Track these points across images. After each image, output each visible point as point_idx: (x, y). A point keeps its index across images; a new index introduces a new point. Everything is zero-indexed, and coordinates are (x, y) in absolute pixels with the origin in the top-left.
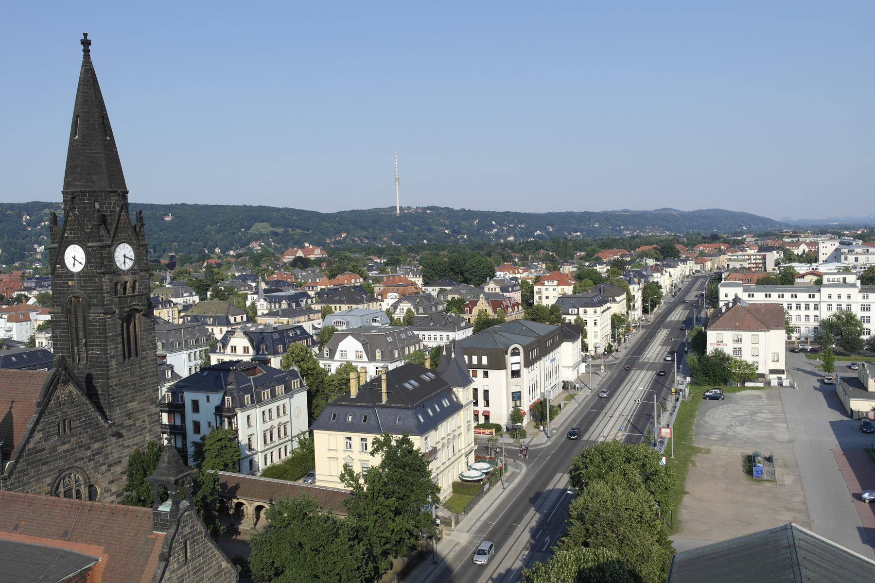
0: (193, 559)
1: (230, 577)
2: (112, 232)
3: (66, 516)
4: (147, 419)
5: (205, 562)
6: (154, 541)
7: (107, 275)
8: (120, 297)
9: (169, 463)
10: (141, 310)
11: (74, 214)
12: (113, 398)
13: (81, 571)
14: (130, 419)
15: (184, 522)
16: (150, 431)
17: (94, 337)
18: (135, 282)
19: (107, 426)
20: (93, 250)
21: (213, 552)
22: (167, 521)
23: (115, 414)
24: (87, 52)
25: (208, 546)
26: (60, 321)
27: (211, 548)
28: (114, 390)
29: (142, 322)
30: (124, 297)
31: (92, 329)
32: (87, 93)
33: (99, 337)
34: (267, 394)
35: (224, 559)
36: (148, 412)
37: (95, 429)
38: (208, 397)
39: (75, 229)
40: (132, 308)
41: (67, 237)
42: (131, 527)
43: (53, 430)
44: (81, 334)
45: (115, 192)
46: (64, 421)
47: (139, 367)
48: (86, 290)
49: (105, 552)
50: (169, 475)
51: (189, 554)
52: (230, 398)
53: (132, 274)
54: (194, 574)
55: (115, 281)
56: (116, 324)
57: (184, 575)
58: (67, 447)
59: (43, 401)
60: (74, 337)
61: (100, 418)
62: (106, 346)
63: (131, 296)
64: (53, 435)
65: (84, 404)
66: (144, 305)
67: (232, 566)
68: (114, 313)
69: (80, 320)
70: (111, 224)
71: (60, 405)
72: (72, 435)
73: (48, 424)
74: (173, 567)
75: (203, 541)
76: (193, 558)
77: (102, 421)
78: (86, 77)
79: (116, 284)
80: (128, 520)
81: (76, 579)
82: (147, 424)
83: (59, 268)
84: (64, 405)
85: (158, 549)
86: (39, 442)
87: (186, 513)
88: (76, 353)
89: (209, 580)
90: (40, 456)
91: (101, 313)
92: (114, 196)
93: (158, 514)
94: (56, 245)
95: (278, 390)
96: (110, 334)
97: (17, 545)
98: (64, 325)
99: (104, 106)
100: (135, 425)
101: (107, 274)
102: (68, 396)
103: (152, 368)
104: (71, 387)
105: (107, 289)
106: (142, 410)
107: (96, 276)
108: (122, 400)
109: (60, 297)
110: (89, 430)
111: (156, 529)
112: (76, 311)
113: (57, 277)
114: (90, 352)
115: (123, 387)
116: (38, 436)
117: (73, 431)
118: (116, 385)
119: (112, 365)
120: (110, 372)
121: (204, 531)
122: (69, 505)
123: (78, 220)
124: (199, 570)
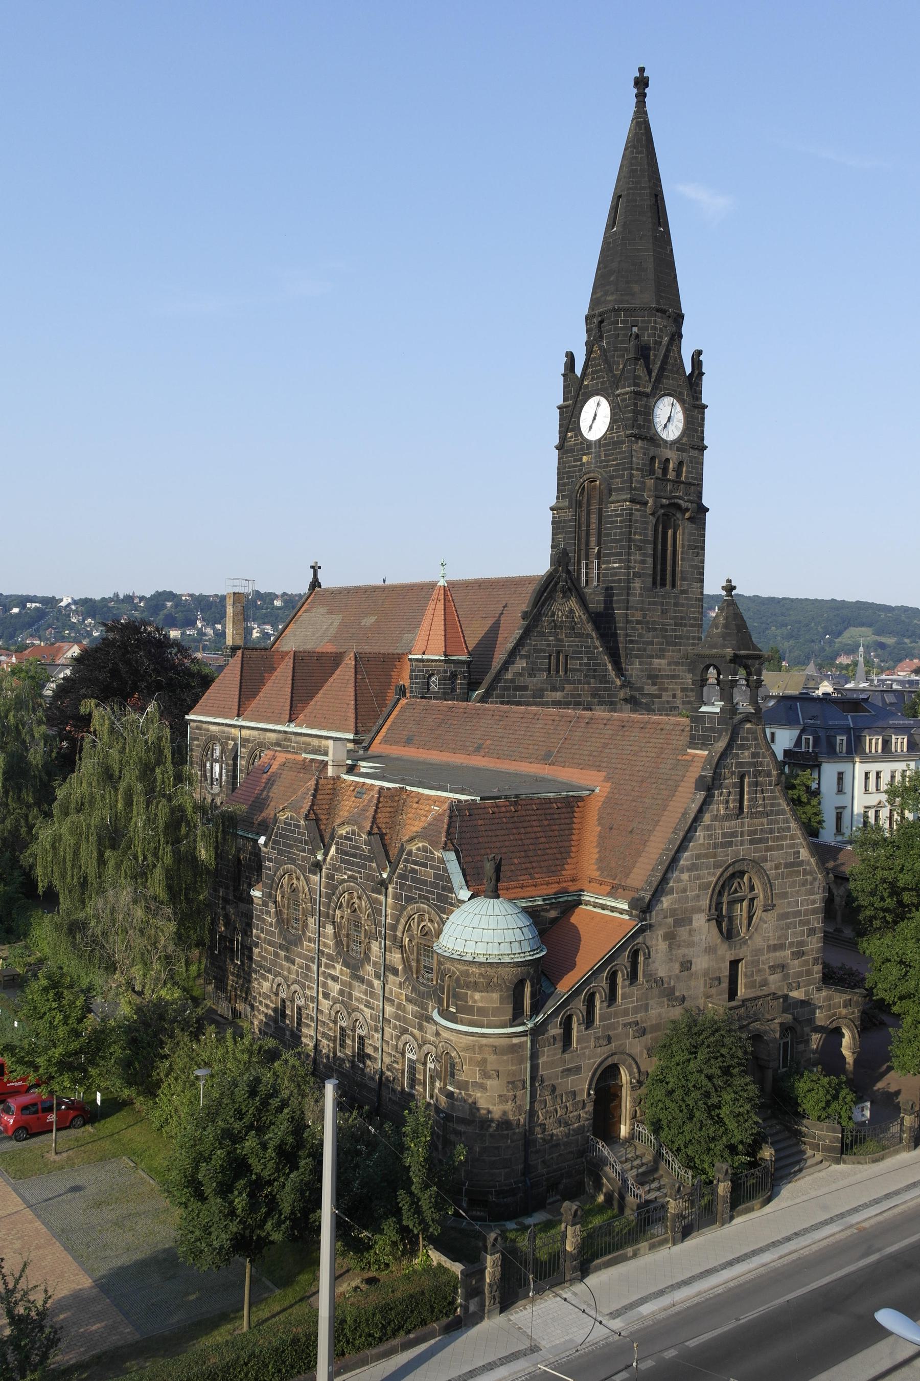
0: (753, 815)
1: (811, 883)
2: (654, 374)
3: (551, 731)
4: (679, 694)
5: (771, 831)
6: (688, 764)
7: (640, 441)
8: (657, 478)
9: (726, 626)
10: (687, 510)
11: (600, 348)
12: (632, 642)
13: (568, 797)
14: (654, 684)
17: (612, 541)
18: (681, 464)
19: (618, 683)
20: (623, 400)
21: (786, 821)
22: (713, 730)
23: (632, 669)
24: (641, 97)
25: (779, 805)
26: (565, 521)
27: (783, 812)
28: (634, 629)
29: (686, 531)
30: (663, 479)
31: (611, 528)
32: (636, 158)
33: (618, 541)
34: (877, 744)
35: (804, 843)
36: (682, 683)
37: (601, 682)
39: (600, 370)
40: (673, 501)
41: (587, 386)
42: (651, 745)
43: (542, 663)
44: (593, 539)
45: (663, 312)
46: (558, 653)
47: (676, 605)
48: (607, 466)
49: (607, 779)
50: (725, 646)
51: (746, 803)
52: (811, 738)
53: (678, 449)
55: (651, 454)
56: (646, 523)
57: (733, 834)
59: (532, 611)
60: (583, 546)
61: (610, 667)
62: (629, 554)
63: (673, 481)
64: (540, 669)
65: (588, 636)
66: (691, 502)
67: (817, 864)
68: (645, 504)
69: (594, 518)
70: (655, 363)
71: (556, 626)
72: (568, 681)
73: (536, 651)
74: (718, 810)
75: (773, 791)
76: (752, 813)
77: (613, 673)
78: (636, 134)
79: (653, 459)
80: (648, 735)
81: (559, 805)
82: (678, 702)
83: (571, 437)
84: (561, 628)
85: (695, 772)
86: (520, 675)
87: (748, 725)
88: (584, 570)
89: (777, 867)
90: (520, 696)
91: (625, 501)
92: (662, 318)
93: (698, 719)
94: (570, 402)
95: (896, 743)
96: (637, 537)
97: (476, 770)
98: (570, 527)
99: (659, 180)
100: (660, 697)
101: (643, 439)
102: (567, 617)
103: (694, 613)
104: (573, 603)
105: (638, 464)
106: (673, 677)
107: (623, 442)
108: (645, 650)
109: (568, 484)
110: (592, 680)
111: (693, 745)
112: (589, 504)
113: (567, 452)
114: (603, 566)
116: (520, 664)
117: (570, 674)
118: (638, 622)
119: (634, 588)
120: (631, 598)
121: (774, 773)
122: (557, 718)
123: (606, 356)
124: (760, 841)
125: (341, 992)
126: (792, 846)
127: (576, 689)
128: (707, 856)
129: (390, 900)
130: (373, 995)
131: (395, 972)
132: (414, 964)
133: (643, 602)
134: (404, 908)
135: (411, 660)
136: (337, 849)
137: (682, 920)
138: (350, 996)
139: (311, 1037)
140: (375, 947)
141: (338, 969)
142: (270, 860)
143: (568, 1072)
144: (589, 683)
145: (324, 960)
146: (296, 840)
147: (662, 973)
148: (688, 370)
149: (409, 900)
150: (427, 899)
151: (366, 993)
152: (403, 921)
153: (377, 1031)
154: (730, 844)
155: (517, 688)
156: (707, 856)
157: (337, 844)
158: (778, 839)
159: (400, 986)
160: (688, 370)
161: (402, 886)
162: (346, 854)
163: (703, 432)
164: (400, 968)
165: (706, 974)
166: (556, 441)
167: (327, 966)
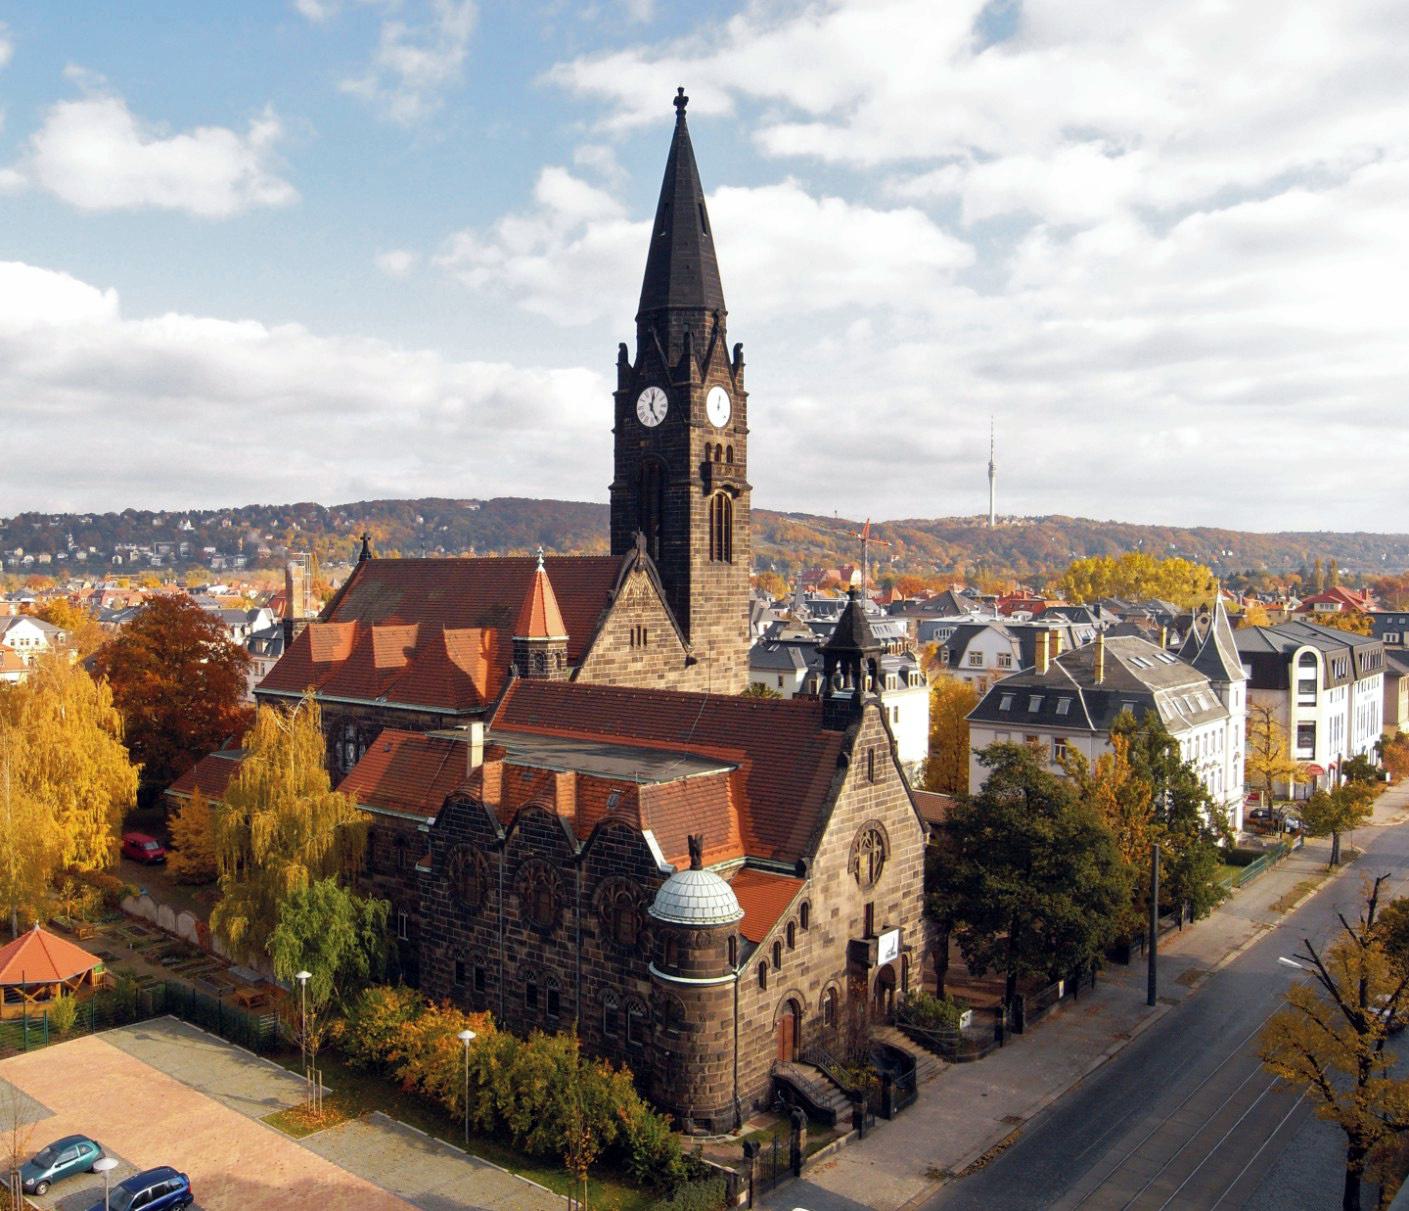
4: (733, 657)
15: (870, 720)
16: (736, 675)
38: (780, 679)
41: (644, 377)
47: (729, 575)
53: (728, 435)
54: (877, 805)
55: (706, 440)
57: (865, 800)
58: (638, 666)
73: (621, 627)
82: (732, 664)
86: (609, 649)
89: (893, 824)
100: (717, 660)
110: (664, 650)
115: (707, 600)
118: (700, 594)
124: (884, 803)
125: (530, 955)
126: (903, 805)
127: (653, 659)
128: (848, 820)
129: (584, 873)
130: (566, 955)
131: (592, 935)
132: (612, 928)
133: (702, 576)
134: (598, 881)
135: (516, 641)
136: (521, 830)
137: (833, 876)
138: (540, 957)
139: (497, 996)
140: (568, 914)
141: (525, 935)
142: (440, 839)
143: (761, 1008)
144: (662, 653)
145: (509, 927)
146: (472, 821)
147: (820, 921)
148: (732, 361)
149: (604, 873)
150: (627, 872)
151: (558, 954)
152: (598, 891)
153: (572, 985)
154: (863, 808)
155: (609, 662)
156: (848, 820)
157: (520, 824)
158: (894, 800)
159: (598, 947)
160: (732, 361)
161: (597, 861)
162: (532, 833)
163: (745, 417)
164: (597, 931)
165: (849, 917)
166: (613, 426)
167: (511, 932)
